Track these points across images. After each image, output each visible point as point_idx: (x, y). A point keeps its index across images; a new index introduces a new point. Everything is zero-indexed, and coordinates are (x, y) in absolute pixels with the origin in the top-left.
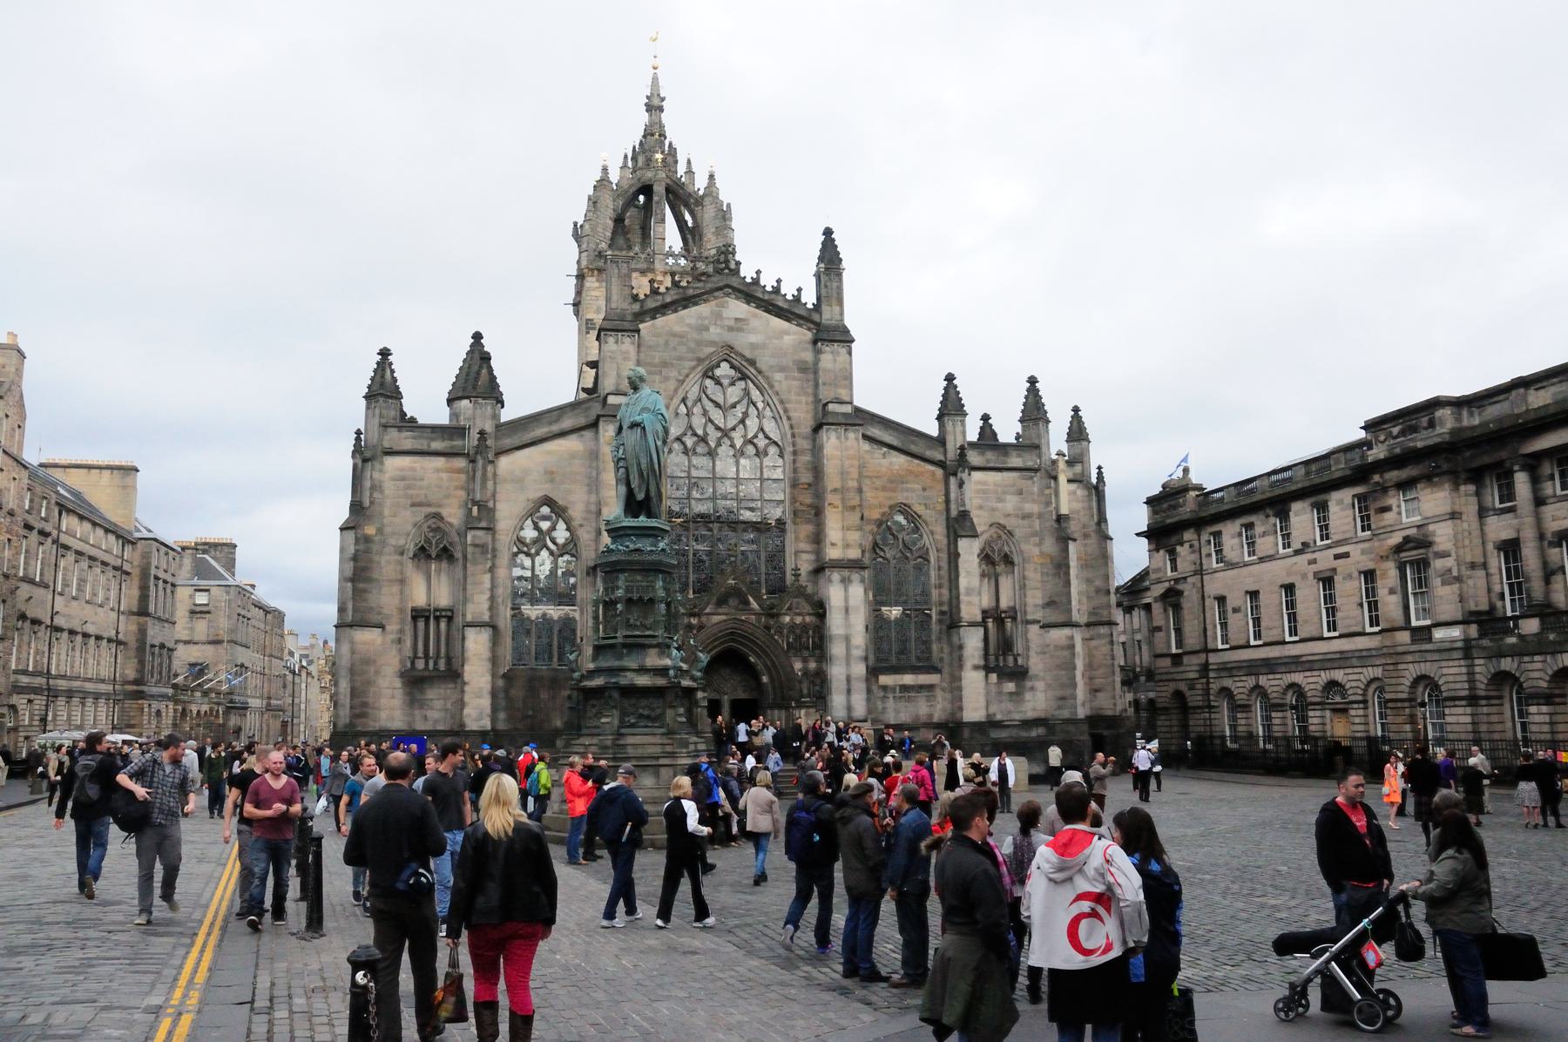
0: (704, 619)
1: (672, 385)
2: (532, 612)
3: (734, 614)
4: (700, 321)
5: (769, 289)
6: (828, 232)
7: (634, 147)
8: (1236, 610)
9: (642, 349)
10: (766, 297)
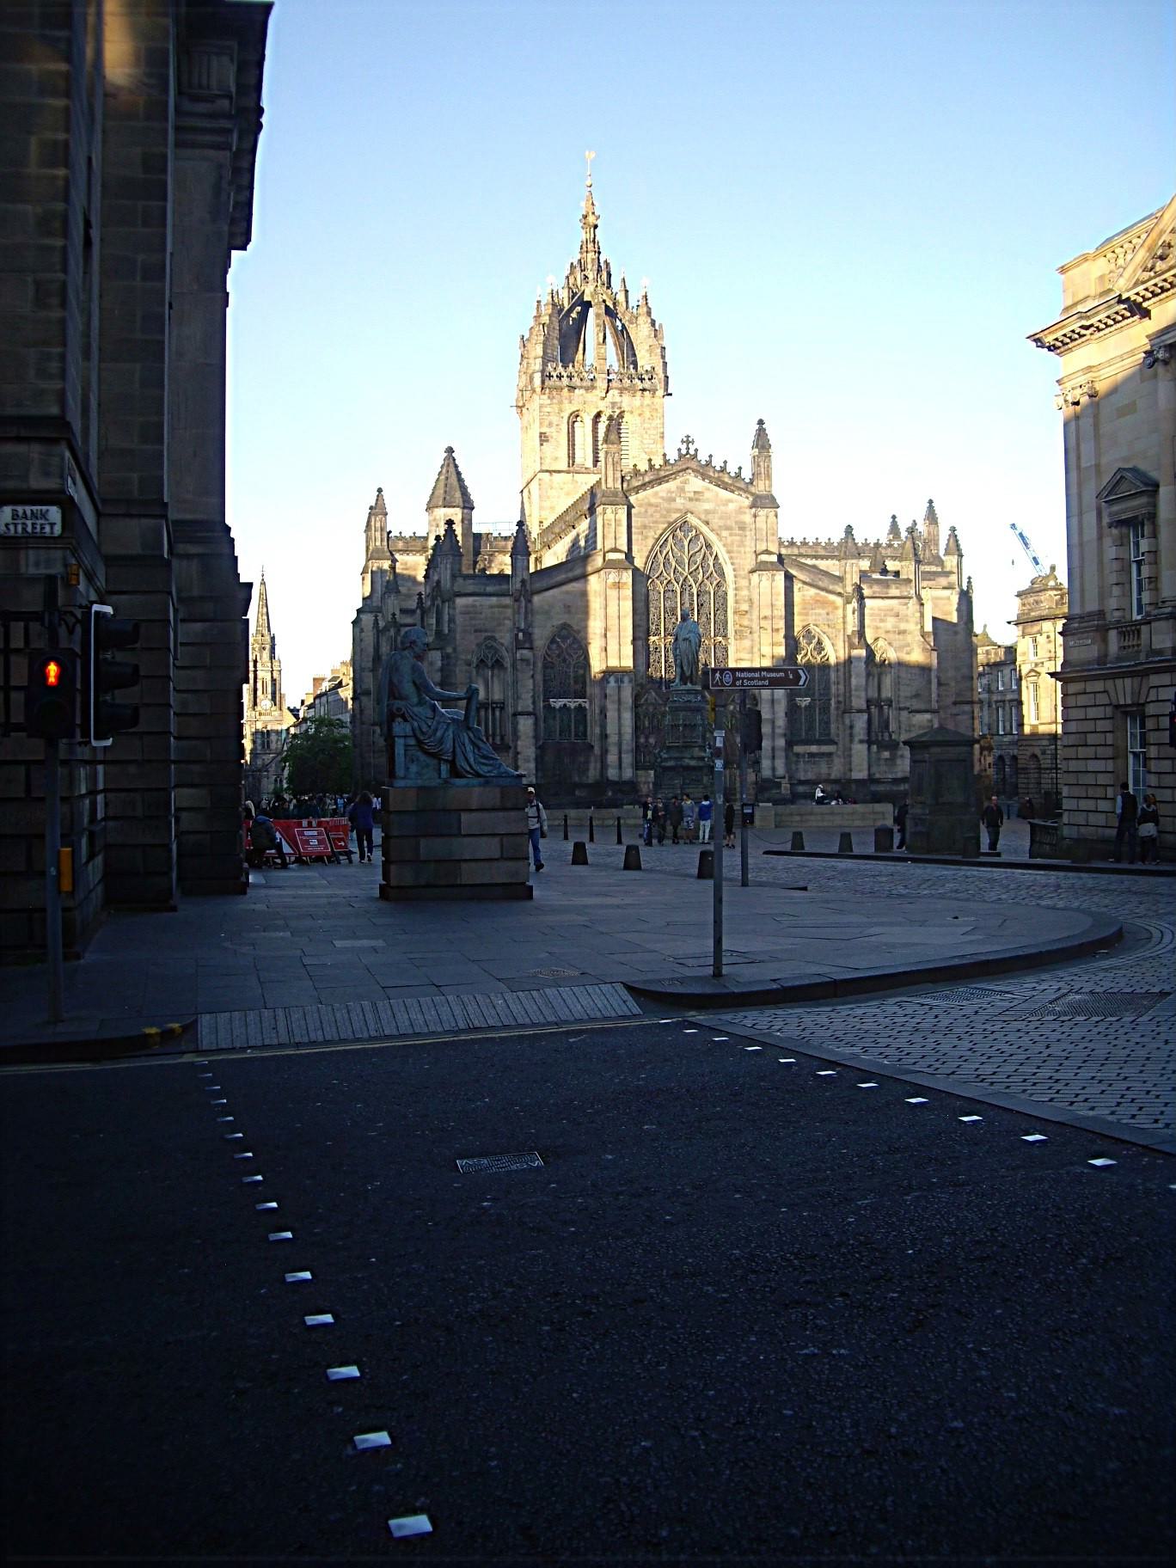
1: (651, 542)
2: (558, 703)
10: (716, 475)
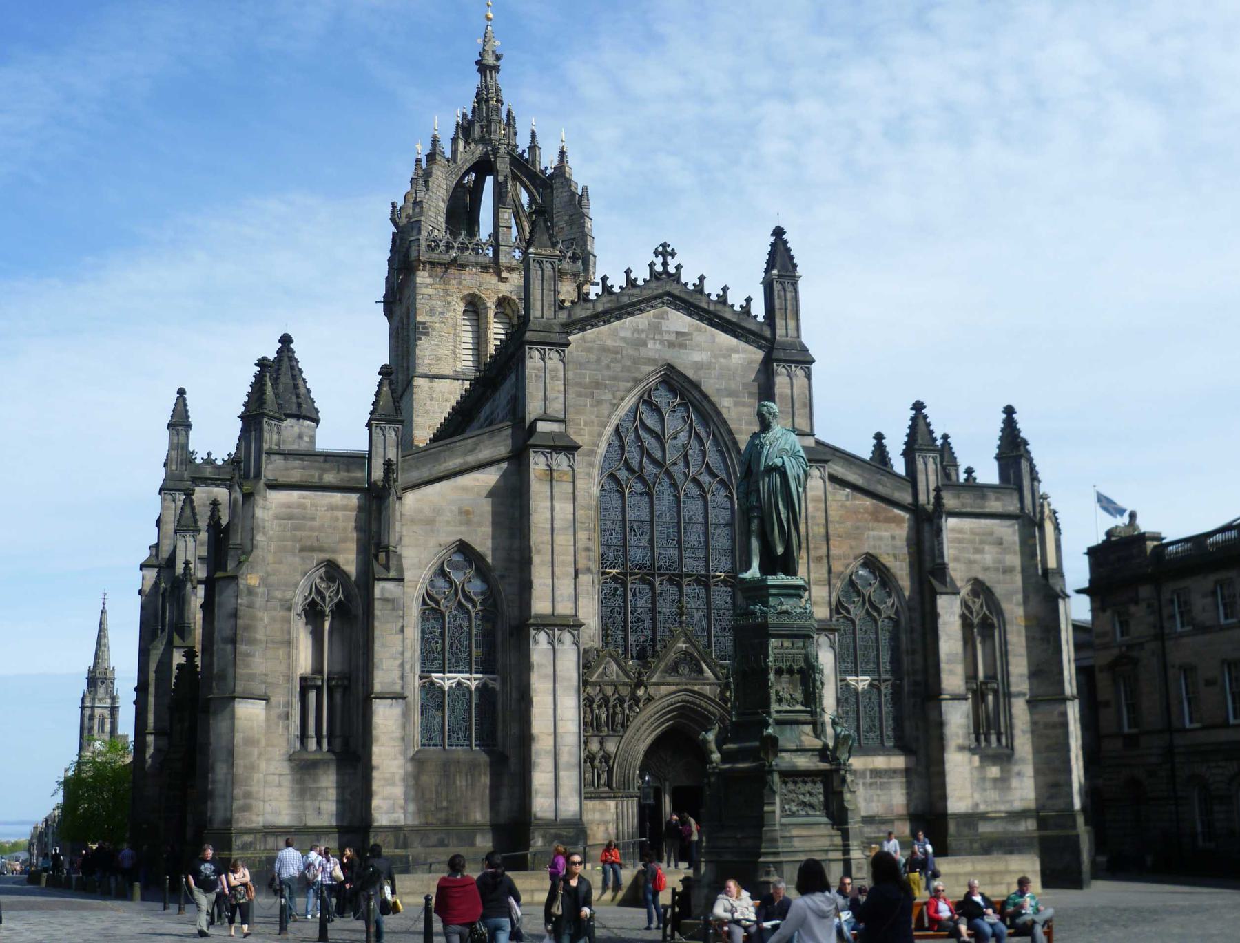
0: (651, 690)
1: (605, 409)
3: (686, 684)
4: (636, 335)
5: (713, 297)
6: (778, 232)
7: (465, 116)
8: (1210, 683)
9: (571, 366)
10: (712, 308)
